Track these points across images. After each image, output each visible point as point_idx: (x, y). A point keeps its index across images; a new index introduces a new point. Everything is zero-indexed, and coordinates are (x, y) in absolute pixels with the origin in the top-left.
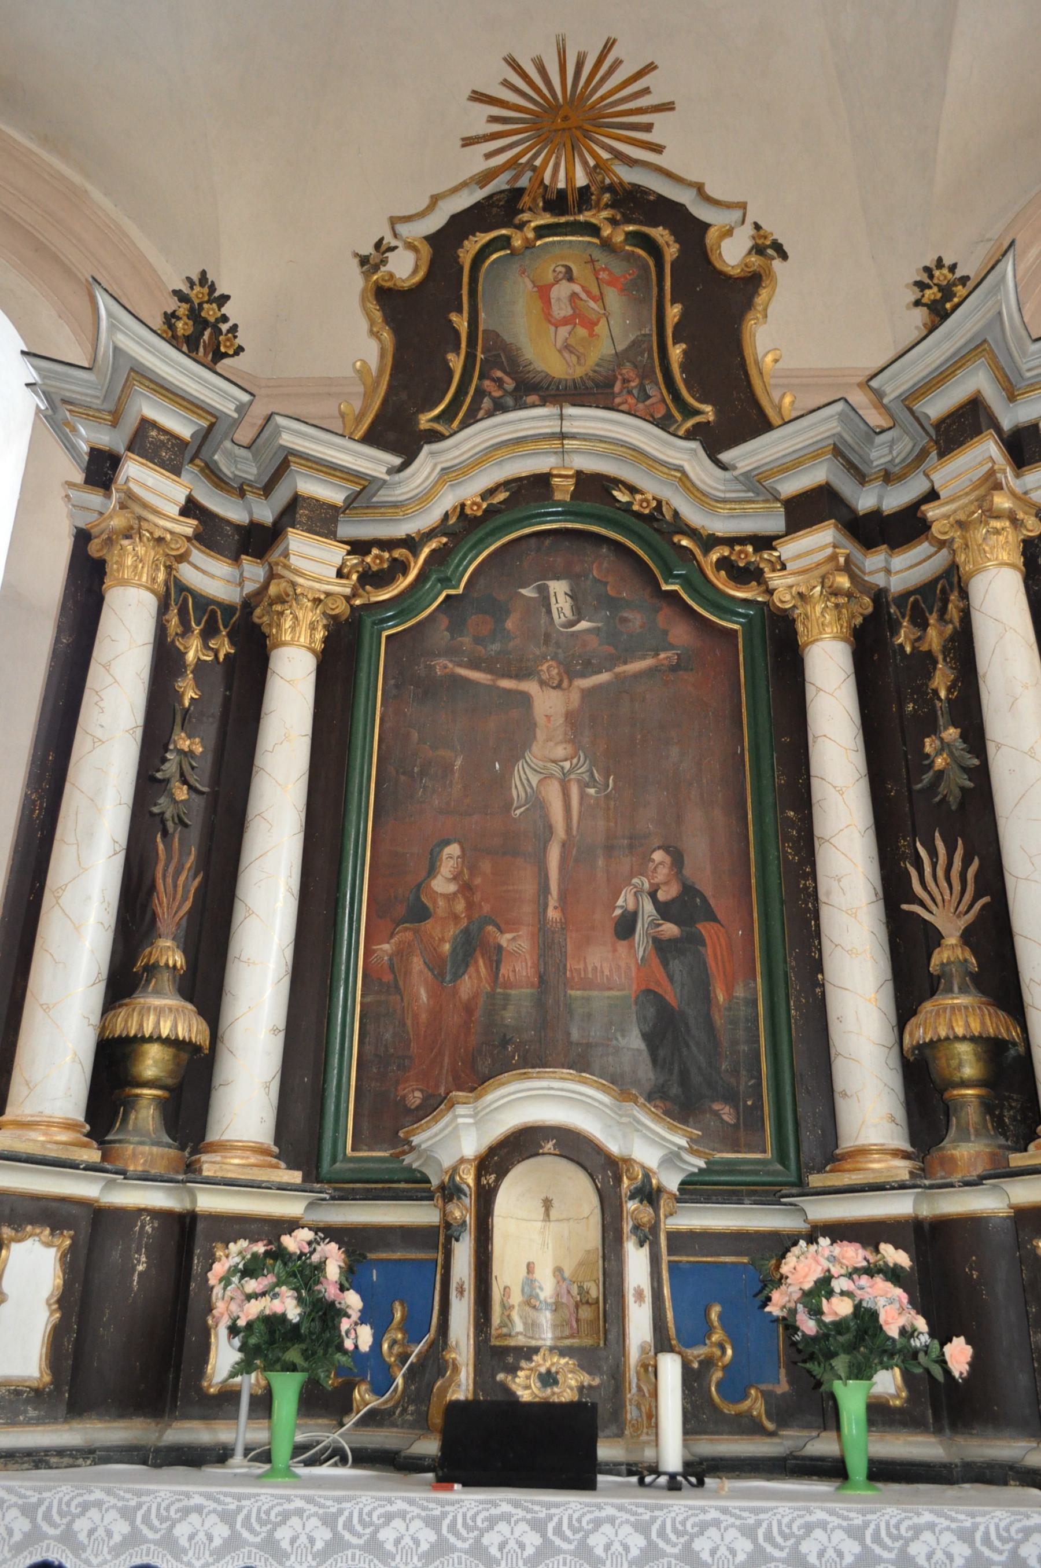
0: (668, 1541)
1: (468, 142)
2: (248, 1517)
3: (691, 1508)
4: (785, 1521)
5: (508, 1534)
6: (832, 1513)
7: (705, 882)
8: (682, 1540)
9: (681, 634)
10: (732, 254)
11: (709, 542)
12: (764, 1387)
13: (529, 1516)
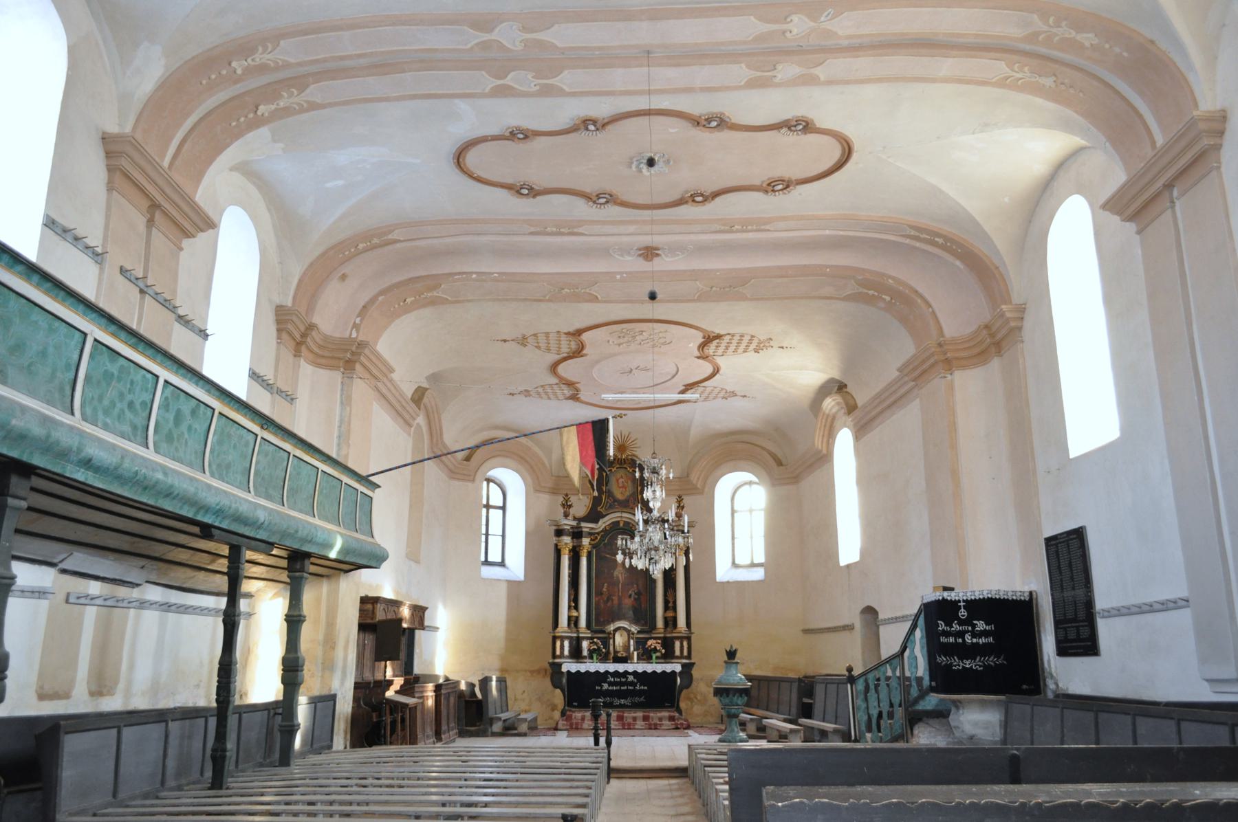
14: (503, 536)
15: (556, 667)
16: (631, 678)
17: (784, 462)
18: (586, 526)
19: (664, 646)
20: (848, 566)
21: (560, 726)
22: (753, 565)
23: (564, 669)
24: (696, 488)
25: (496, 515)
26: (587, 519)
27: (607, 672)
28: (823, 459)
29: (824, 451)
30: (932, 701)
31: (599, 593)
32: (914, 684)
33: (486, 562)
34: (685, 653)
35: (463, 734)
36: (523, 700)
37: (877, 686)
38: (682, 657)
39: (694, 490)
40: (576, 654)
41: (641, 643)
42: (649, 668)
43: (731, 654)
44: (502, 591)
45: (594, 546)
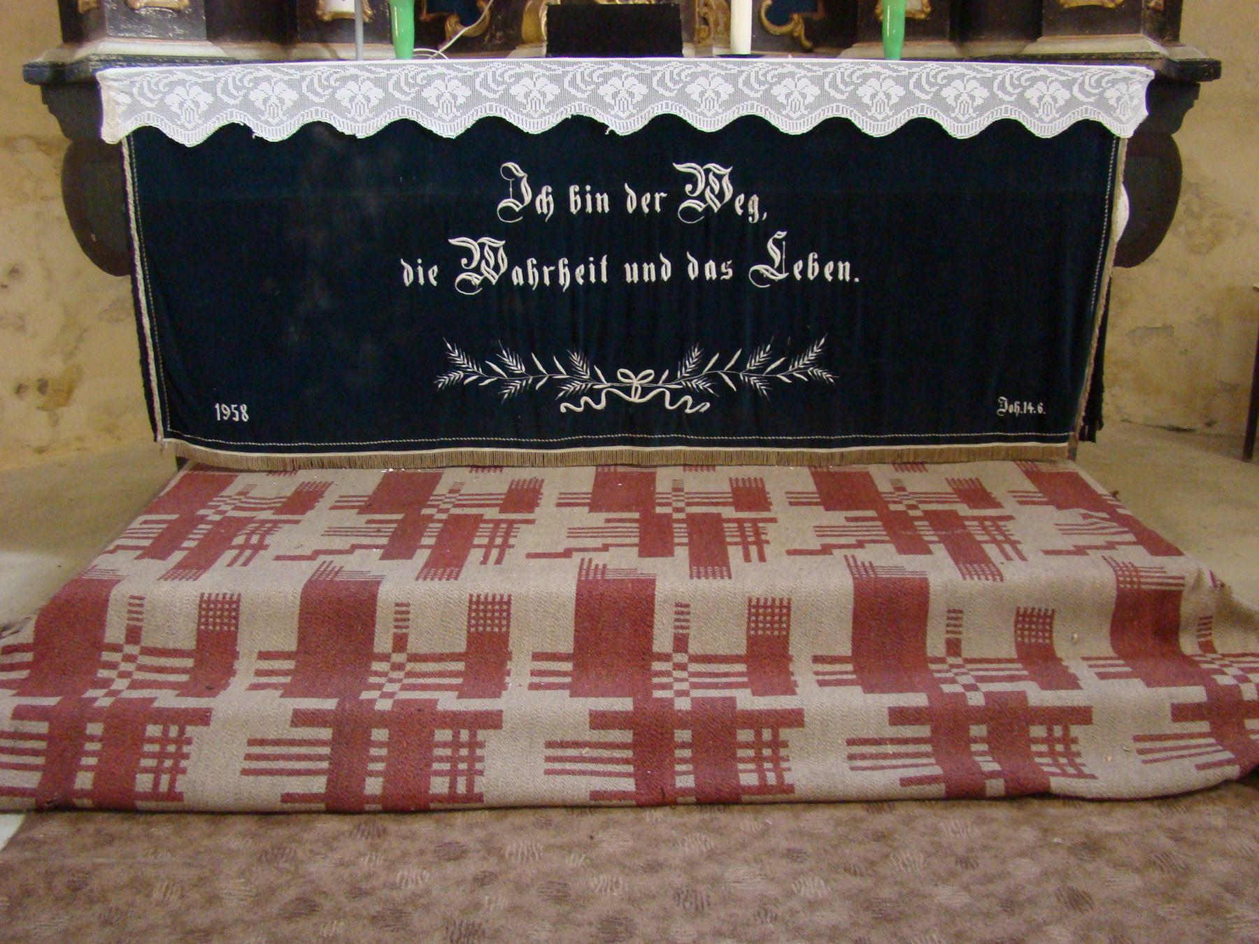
0: (752, 89)
2: (397, 83)
3: (772, 64)
4: (847, 73)
5: (620, 87)
6: (884, 67)
8: (763, 88)
12: (808, 14)
13: (637, 73)
16: (710, 186)
27: (493, 136)
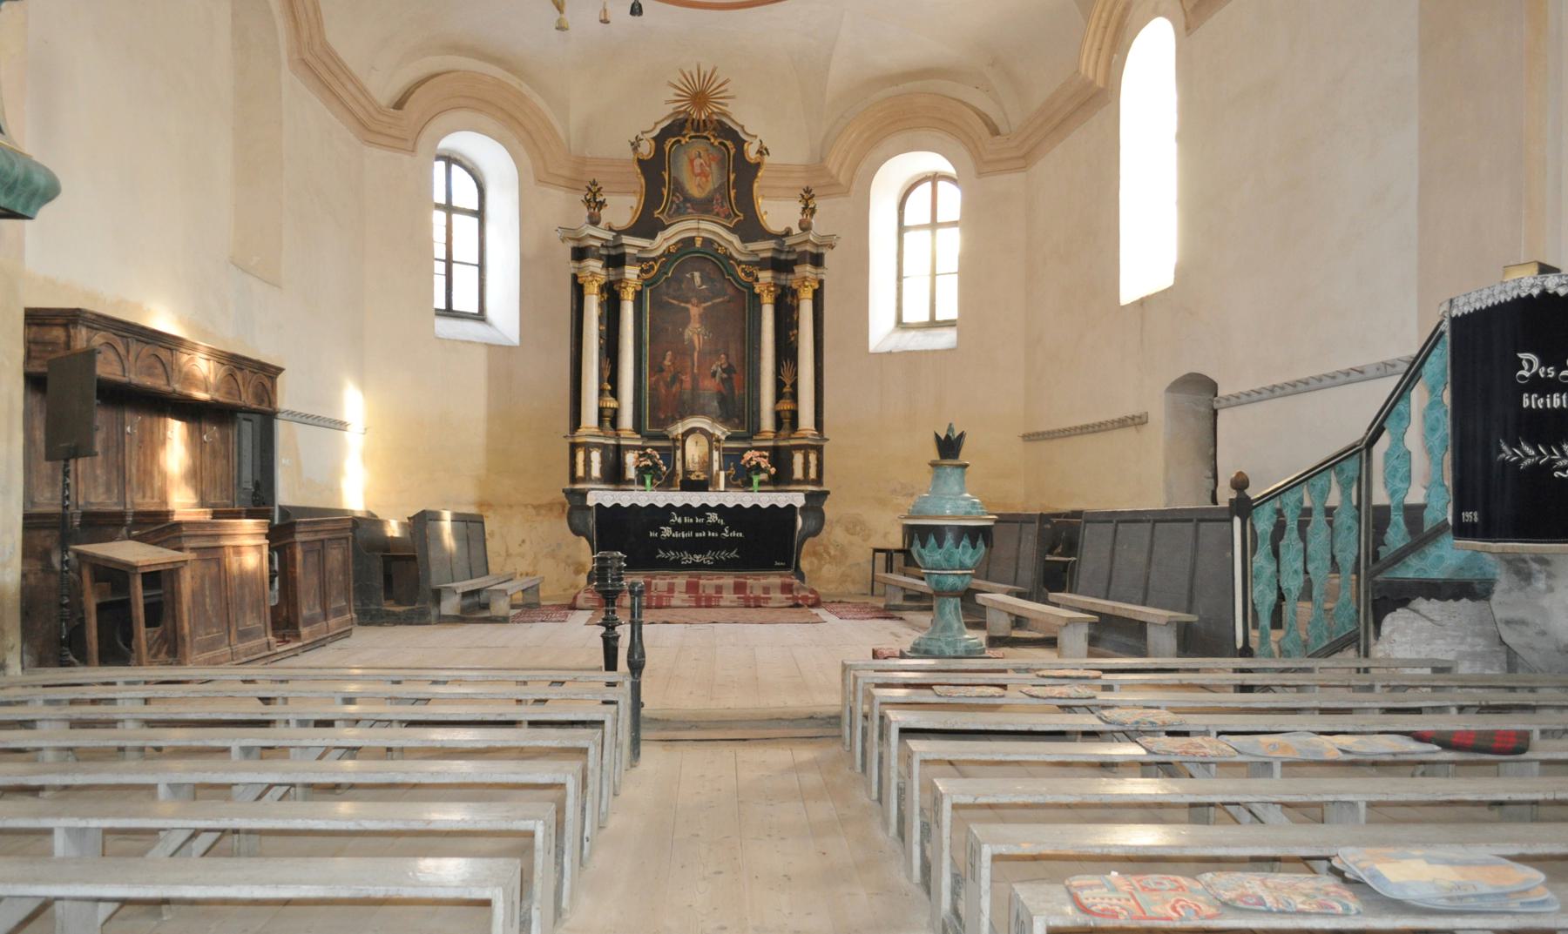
1: (667, 102)
7: (734, 362)
9: (730, 291)
10: (751, 153)
11: (739, 263)
14: (481, 266)
15: (576, 499)
16: (713, 517)
17: (1003, 128)
18: (633, 244)
19: (774, 461)
20: (1142, 303)
21: (580, 602)
22: (933, 324)
23: (592, 500)
24: (837, 184)
25: (466, 228)
26: (633, 231)
27: (670, 507)
28: (1094, 100)
29: (1100, 83)
30: (1449, 557)
31: (657, 369)
32: (1397, 518)
33: (449, 312)
34: (813, 474)
35: (370, 617)
36: (522, 556)
37: (1303, 526)
38: (806, 480)
39: (835, 188)
40: (614, 475)
41: (732, 458)
42: (746, 499)
43: (949, 447)
44: (478, 366)
45: (647, 283)
